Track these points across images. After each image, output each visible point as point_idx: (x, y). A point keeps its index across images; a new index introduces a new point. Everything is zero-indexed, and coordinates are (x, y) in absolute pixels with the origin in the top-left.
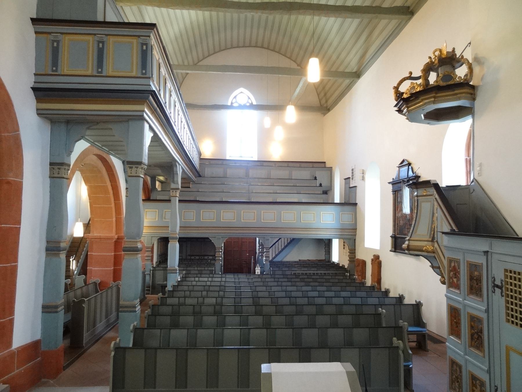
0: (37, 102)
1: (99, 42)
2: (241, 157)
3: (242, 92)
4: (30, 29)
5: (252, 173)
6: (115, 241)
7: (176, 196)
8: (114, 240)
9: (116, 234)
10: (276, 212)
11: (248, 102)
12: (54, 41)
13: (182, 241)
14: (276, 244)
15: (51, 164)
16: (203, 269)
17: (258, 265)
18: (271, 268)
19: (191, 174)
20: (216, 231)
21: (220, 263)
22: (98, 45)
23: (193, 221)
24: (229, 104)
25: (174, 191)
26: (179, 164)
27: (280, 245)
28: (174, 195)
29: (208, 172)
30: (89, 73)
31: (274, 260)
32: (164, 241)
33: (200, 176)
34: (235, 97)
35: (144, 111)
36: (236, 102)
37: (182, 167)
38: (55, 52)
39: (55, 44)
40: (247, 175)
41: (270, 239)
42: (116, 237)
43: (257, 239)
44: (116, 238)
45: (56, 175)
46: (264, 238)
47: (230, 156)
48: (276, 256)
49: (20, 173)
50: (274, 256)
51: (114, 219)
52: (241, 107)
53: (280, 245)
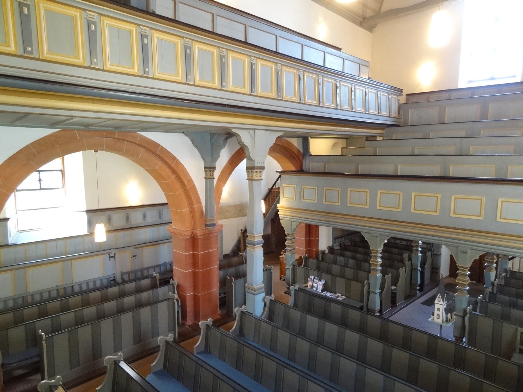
2: (492, 79)
10: (484, 199)
17: (439, 294)
20: (370, 223)
23: (337, 205)
29: (413, 115)
40: (484, 116)
41: (469, 251)
46: (457, 247)
47: (470, 82)
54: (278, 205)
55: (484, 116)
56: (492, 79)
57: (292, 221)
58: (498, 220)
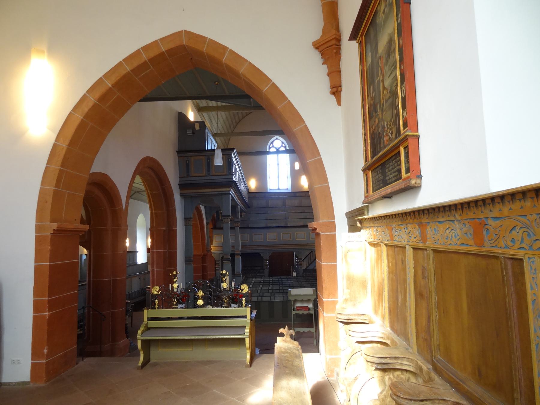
0: (180, 190)
1: (208, 159)
3: (277, 139)
4: (176, 155)
5: (289, 203)
6: (202, 257)
7: (239, 227)
8: (202, 256)
9: (202, 253)
11: (282, 146)
12: (187, 161)
13: (243, 255)
14: (309, 256)
15: (185, 219)
16: (256, 275)
17: (294, 271)
18: (304, 273)
19: (243, 207)
21: (267, 271)
22: (208, 161)
24: (268, 150)
25: (237, 223)
26: (239, 206)
27: (312, 257)
28: (237, 226)
29: (255, 203)
30: (204, 174)
31: (308, 268)
32: (233, 255)
33: (249, 207)
34: (272, 143)
35: (230, 191)
36: (273, 146)
37: (240, 207)
38: (188, 166)
39: (188, 162)
40: (284, 205)
42: (203, 254)
43: (294, 253)
44: (203, 255)
45: (187, 224)
48: (309, 265)
49: (176, 226)
50: (307, 265)
51: (201, 243)
52: (278, 152)
53: (312, 257)
54: (211, 246)
55: (284, 205)
56: (279, 189)
57: (220, 254)
58: (310, 239)
